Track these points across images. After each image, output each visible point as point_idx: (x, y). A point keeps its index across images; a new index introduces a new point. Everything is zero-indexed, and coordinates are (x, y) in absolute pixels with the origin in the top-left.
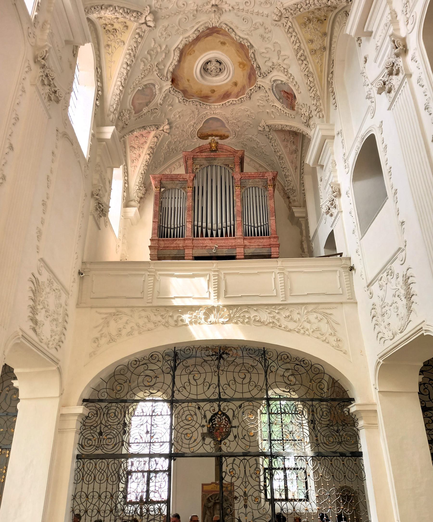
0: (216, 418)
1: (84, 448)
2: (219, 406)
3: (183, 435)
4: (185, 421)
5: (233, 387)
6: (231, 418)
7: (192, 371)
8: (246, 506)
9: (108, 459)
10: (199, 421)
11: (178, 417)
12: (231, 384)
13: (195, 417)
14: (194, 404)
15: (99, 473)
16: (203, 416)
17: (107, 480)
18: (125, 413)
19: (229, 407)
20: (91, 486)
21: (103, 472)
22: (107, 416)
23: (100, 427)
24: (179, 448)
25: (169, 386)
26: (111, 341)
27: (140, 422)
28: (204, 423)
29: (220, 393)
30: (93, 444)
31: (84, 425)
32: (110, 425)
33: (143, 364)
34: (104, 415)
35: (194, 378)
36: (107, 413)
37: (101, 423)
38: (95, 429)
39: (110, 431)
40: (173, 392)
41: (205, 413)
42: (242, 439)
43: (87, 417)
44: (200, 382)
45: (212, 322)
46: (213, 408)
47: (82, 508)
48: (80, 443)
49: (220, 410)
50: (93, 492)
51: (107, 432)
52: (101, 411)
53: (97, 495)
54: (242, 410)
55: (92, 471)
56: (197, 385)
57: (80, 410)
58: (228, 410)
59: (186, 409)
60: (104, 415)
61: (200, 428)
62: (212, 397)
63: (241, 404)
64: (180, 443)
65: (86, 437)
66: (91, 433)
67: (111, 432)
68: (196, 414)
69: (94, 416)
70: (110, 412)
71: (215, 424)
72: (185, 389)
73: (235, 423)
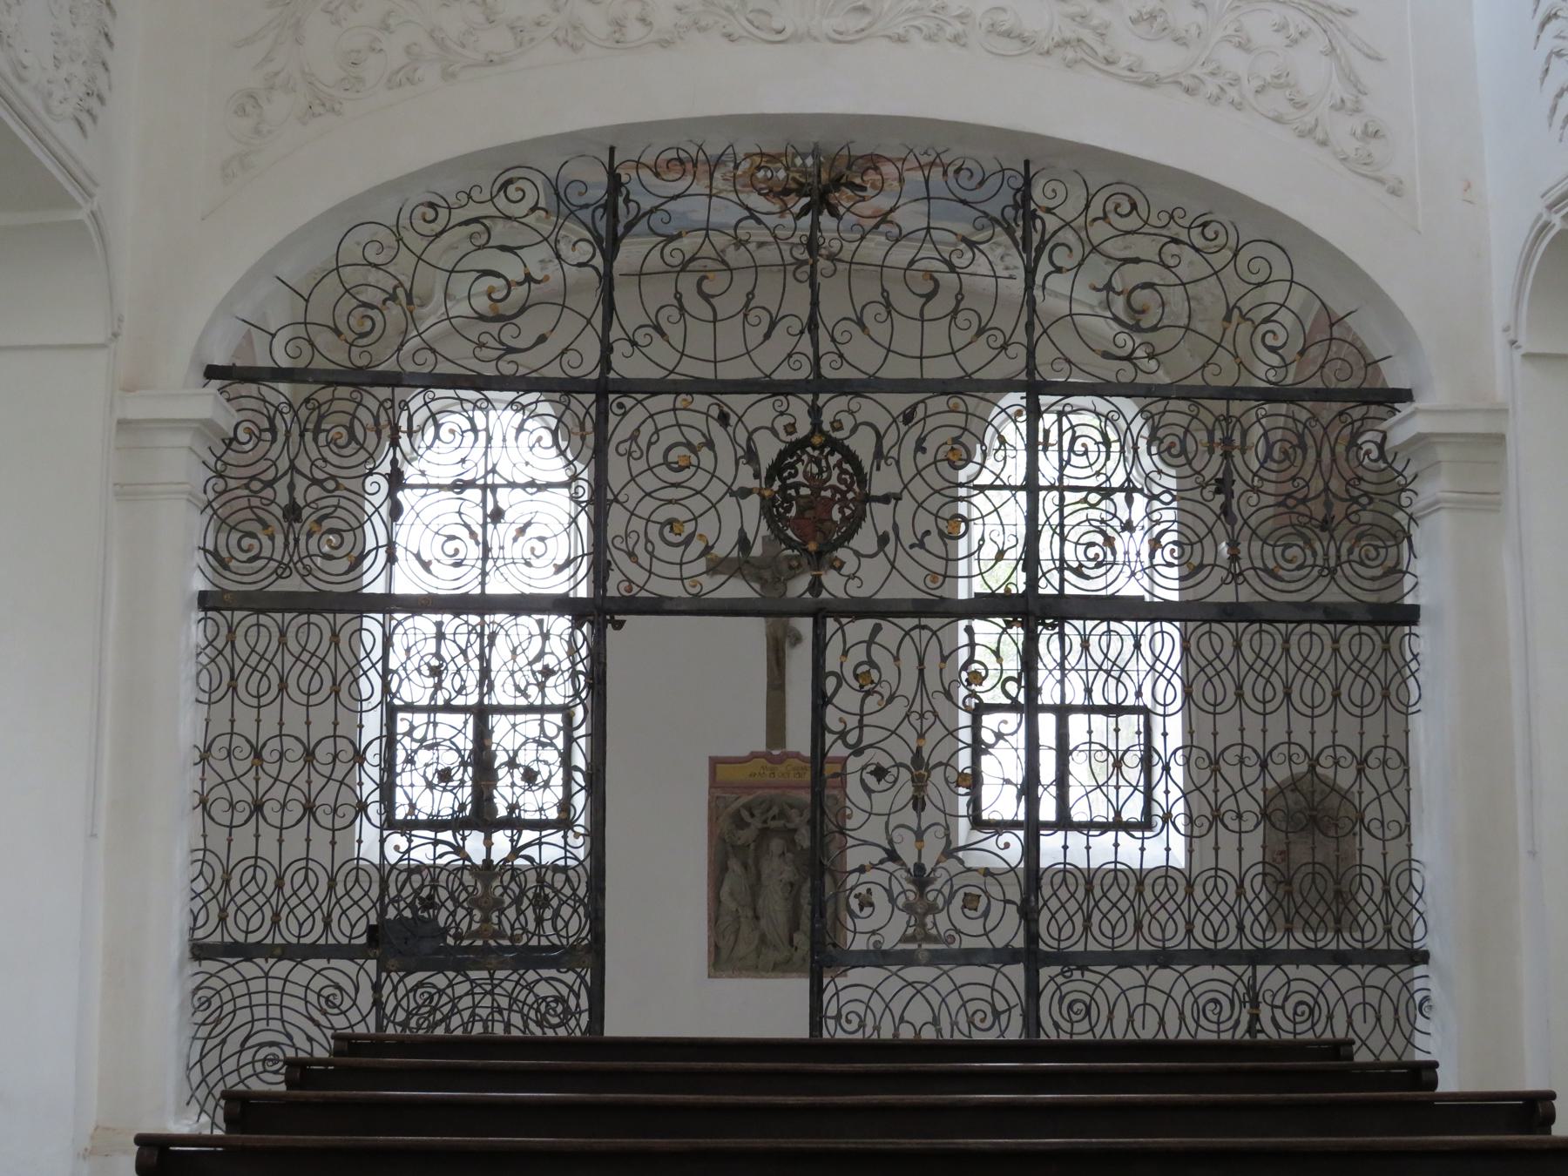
0: (800, 460)
1: (226, 567)
2: (815, 412)
3: (654, 530)
4: (663, 471)
5: (880, 331)
6: (867, 464)
7: (693, 259)
8: (918, 804)
9: (334, 612)
10: (726, 470)
11: (629, 454)
12: (868, 319)
13: (705, 454)
14: (702, 401)
15: (300, 665)
16: (740, 453)
17: (337, 694)
18: (396, 429)
19: (860, 418)
20: (270, 715)
21: (315, 662)
23: (291, 487)
24: (639, 576)
25: (589, 322)
26: (318, 109)
27: (459, 469)
28: (746, 478)
29: (817, 358)
31: (220, 475)
32: (333, 477)
33: (467, 223)
34: (302, 435)
35: (700, 292)
38: (268, 493)
39: (334, 501)
40: (607, 349)
41: (750, 439)
42: (912, 546)
43: (230, 442)
44: (730, 304)
45: (789, 31)
46: (786, 420)
47: (239, 793)
48: (210, 546)
49: (817, 426)
50: (281, 735)
51: (322, 503)
53: (299, 750)
54: (915, 432)
55: (269, 656)
56: (715, 321)
57: (208, 404)
58: (854, 430)
59: (669, 418)
61: (730, 502)
62: (784, 374)
63: (914, 407)
64: (644, 558)
65: (231, 521)
66: (251, 508)
67: (337, 507)
68: (710, 444)
71: (797, 486)
72: (663, 334)
73: (882, 482)
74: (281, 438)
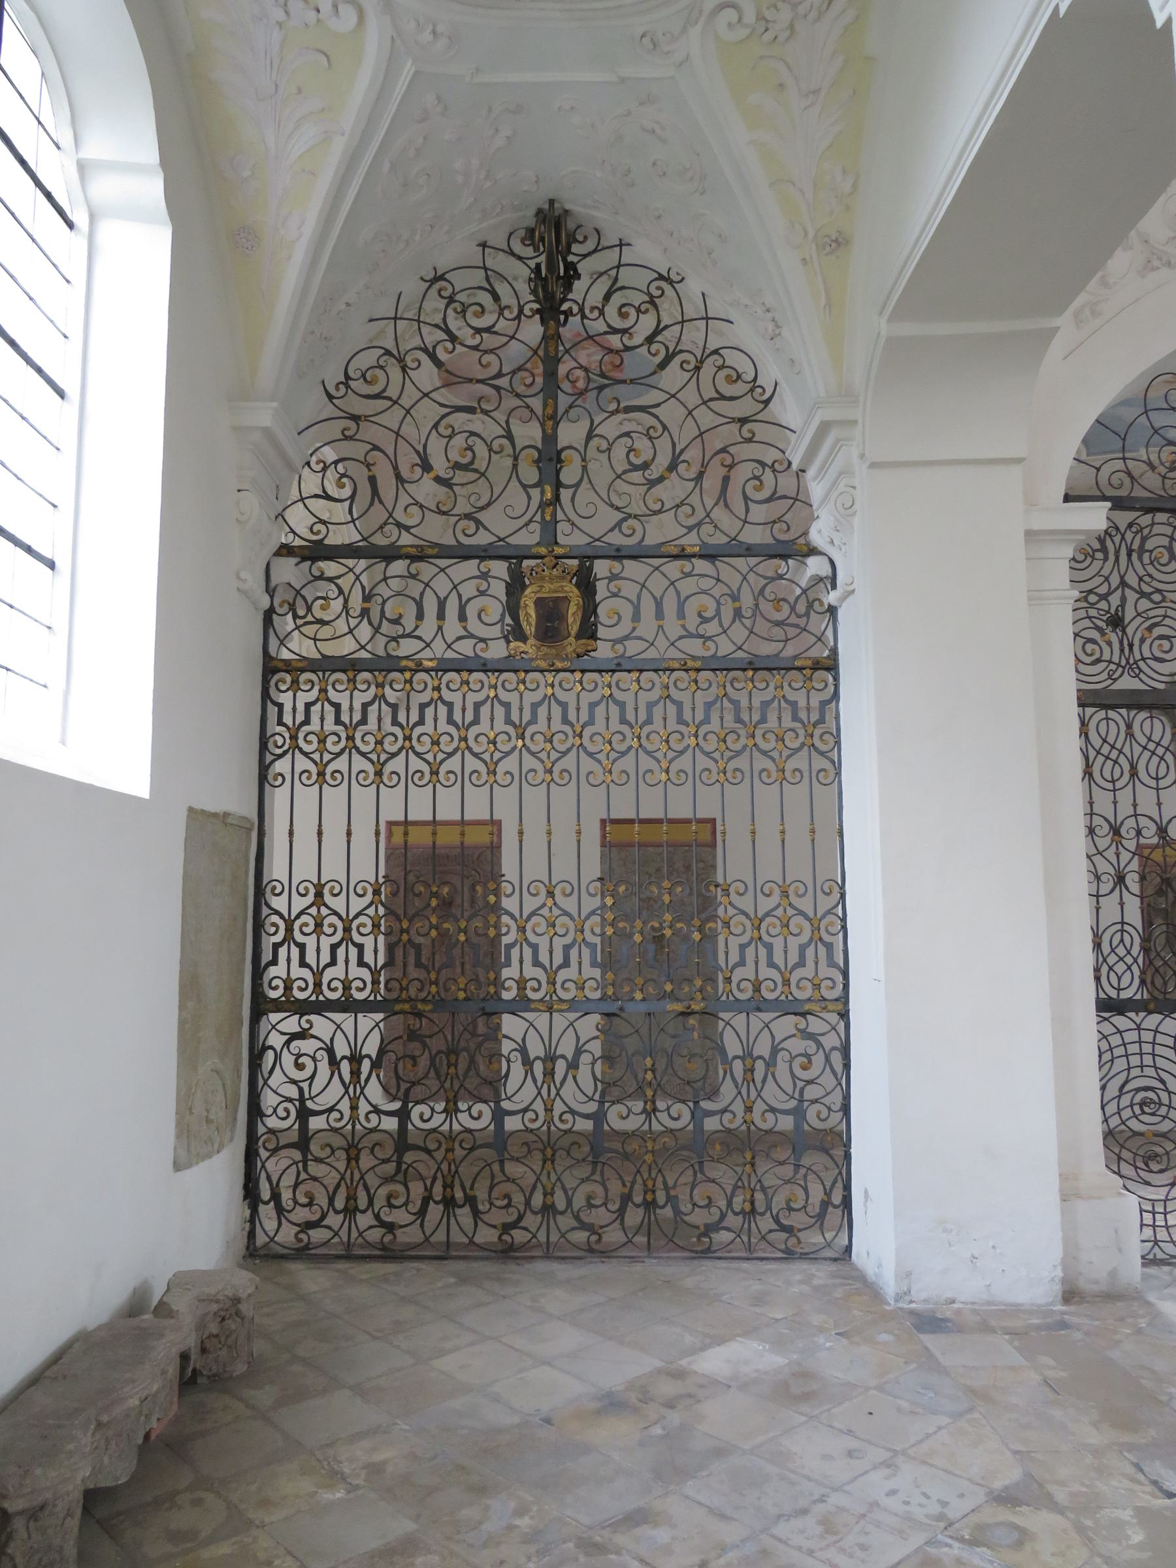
20: (1125, 797)
21: (1160, 751)
22: (1140, 559)
30: (1106, 656)
32: (1159, 591)
36: (1142, 550)
37: (1123, 584)
39: (1161, 612)
51: (1151, 613)
52: (1117, 539)
55: (1118, 746)
60: (1129, 555)
66: (1089, 618)
67: (1165, 616)
69: (1093, 558)
70: (1149, 545)
74: (1112, 557)
